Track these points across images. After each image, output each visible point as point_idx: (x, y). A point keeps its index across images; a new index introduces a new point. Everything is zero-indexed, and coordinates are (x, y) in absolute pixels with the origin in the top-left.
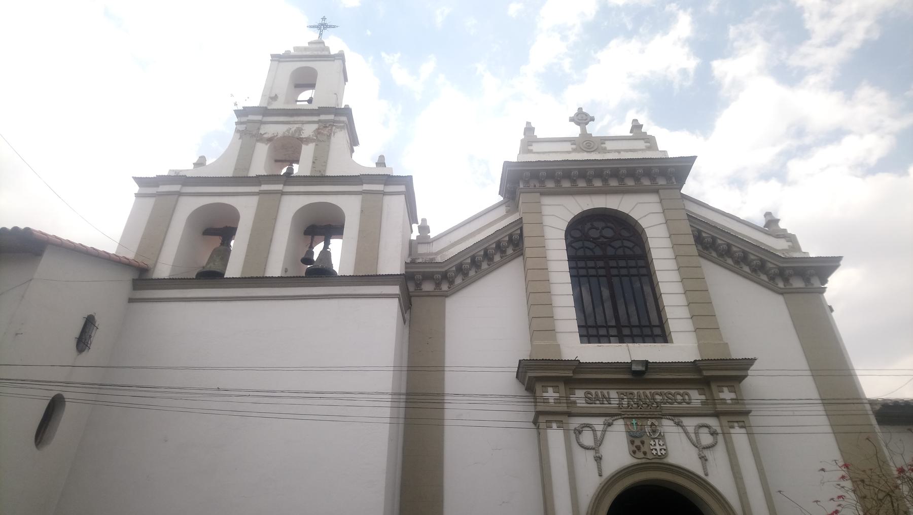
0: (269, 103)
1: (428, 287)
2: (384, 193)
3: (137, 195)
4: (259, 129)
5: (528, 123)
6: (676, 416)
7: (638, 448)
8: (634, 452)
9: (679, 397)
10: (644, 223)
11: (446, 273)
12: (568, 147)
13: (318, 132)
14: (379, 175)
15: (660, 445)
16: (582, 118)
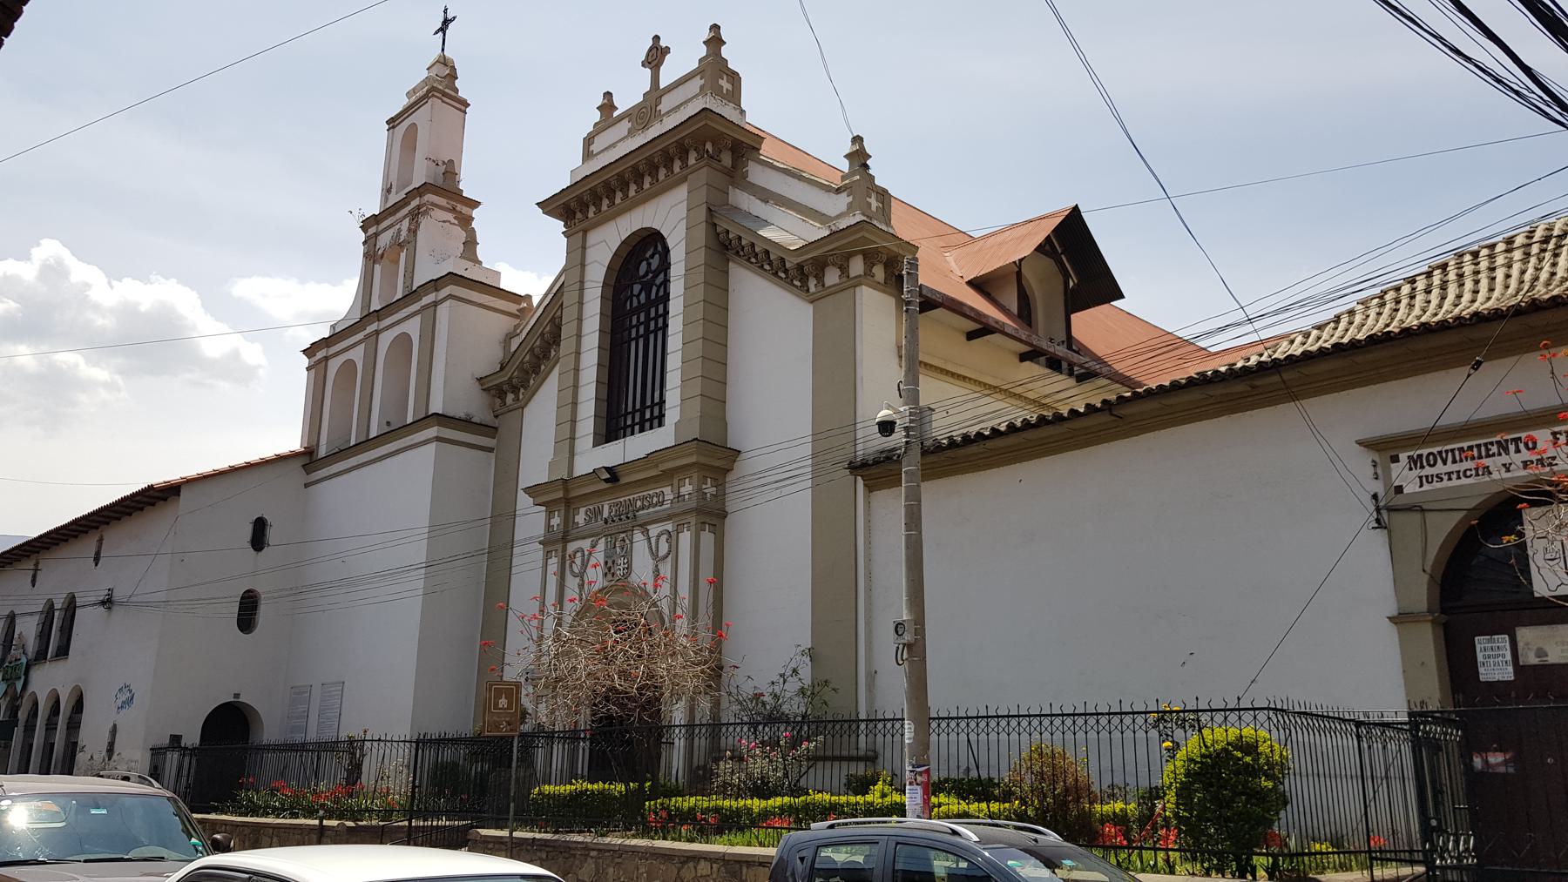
0: (386, 200)
1: (510, 397)
2: (435, 304)
3: (308, 369)
4: (375, 245)
5: (608, 95)
6: (644, 527)
7: (609, 569)
8: (606, 574)
9: (655, 499)
10: (670, 243)
11: (511, 378)
12: (625, 125)
13: (409, 230)
14: (428, 283)
15: (624, 564)
16: (656, 55)
